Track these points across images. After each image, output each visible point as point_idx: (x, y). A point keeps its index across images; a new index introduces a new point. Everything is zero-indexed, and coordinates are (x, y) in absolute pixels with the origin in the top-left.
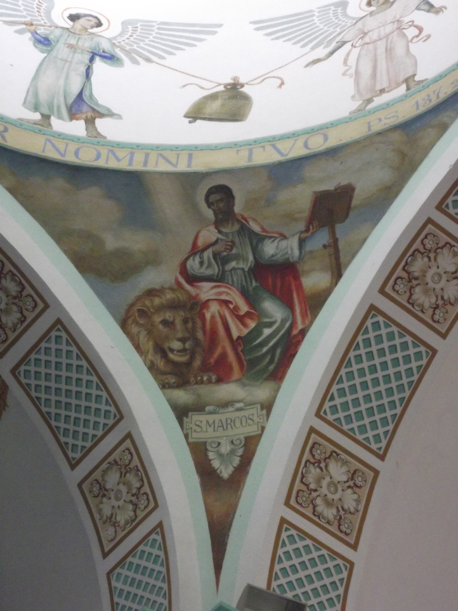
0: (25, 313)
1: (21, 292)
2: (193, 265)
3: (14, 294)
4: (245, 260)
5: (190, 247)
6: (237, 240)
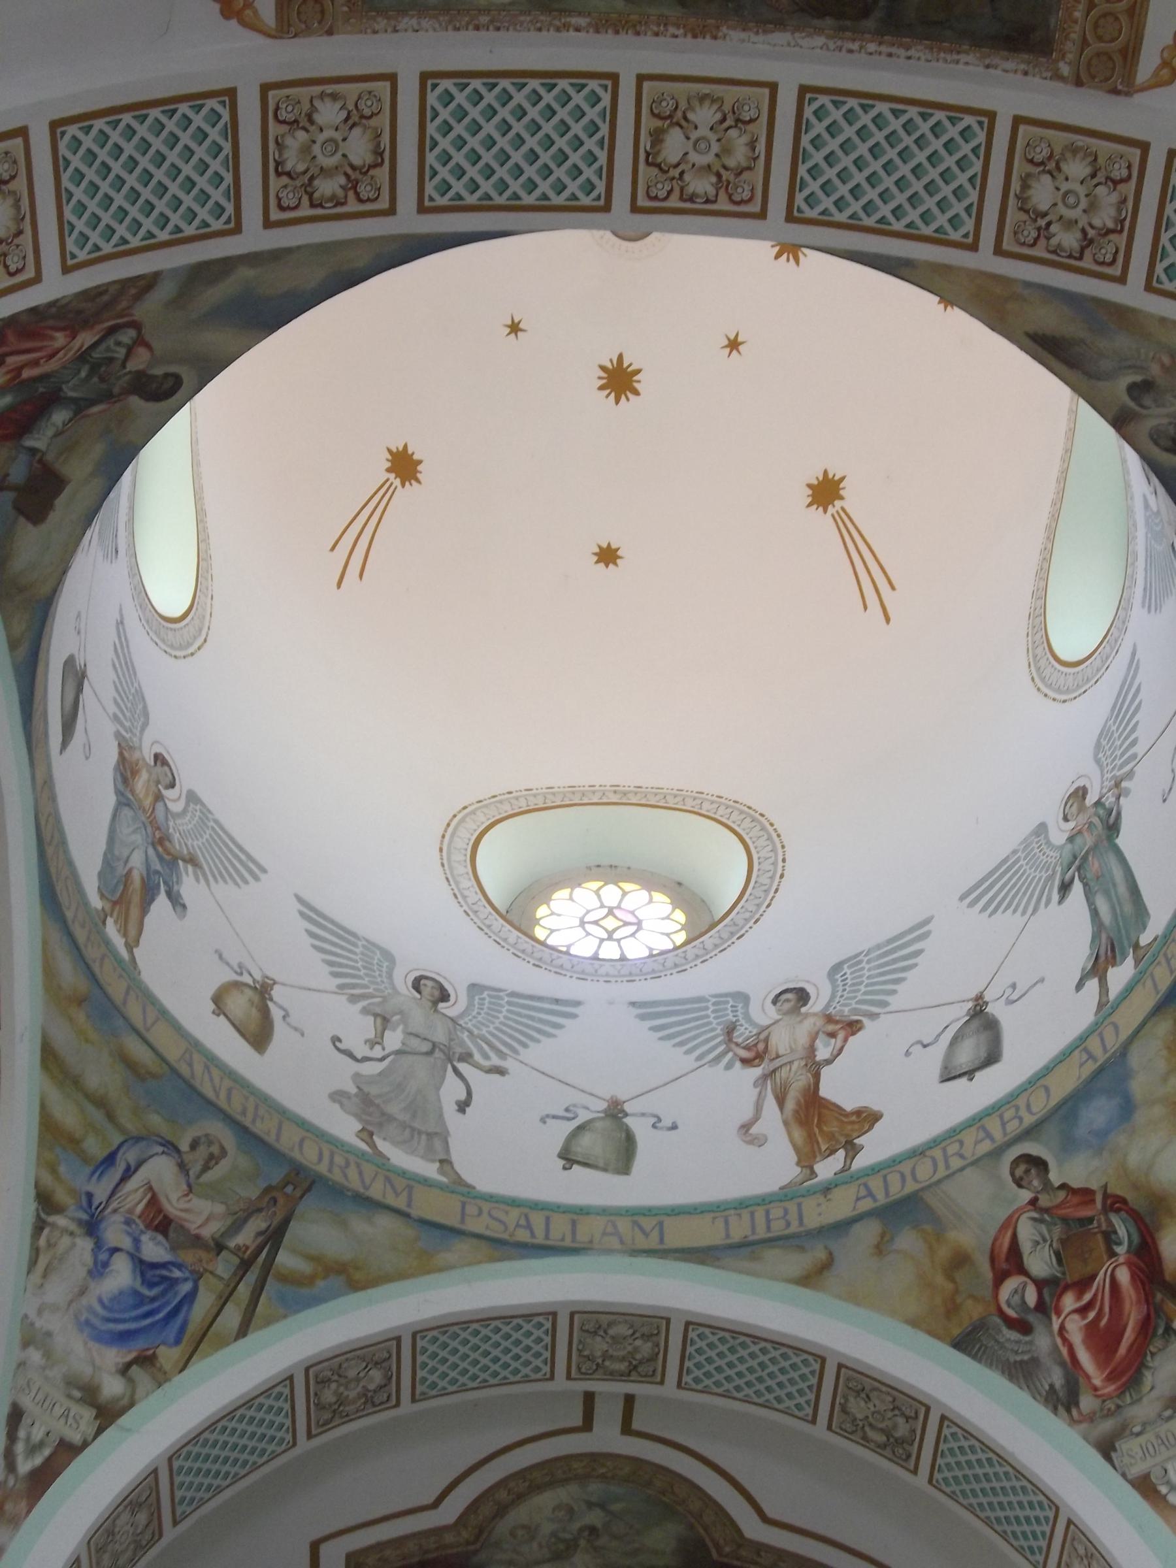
0: (285, 180)
1: (311, 195)
2: (127, 336)
3: (316, 183)
4: (73, 389)
5: (147, 338)
6: (104, 386)
